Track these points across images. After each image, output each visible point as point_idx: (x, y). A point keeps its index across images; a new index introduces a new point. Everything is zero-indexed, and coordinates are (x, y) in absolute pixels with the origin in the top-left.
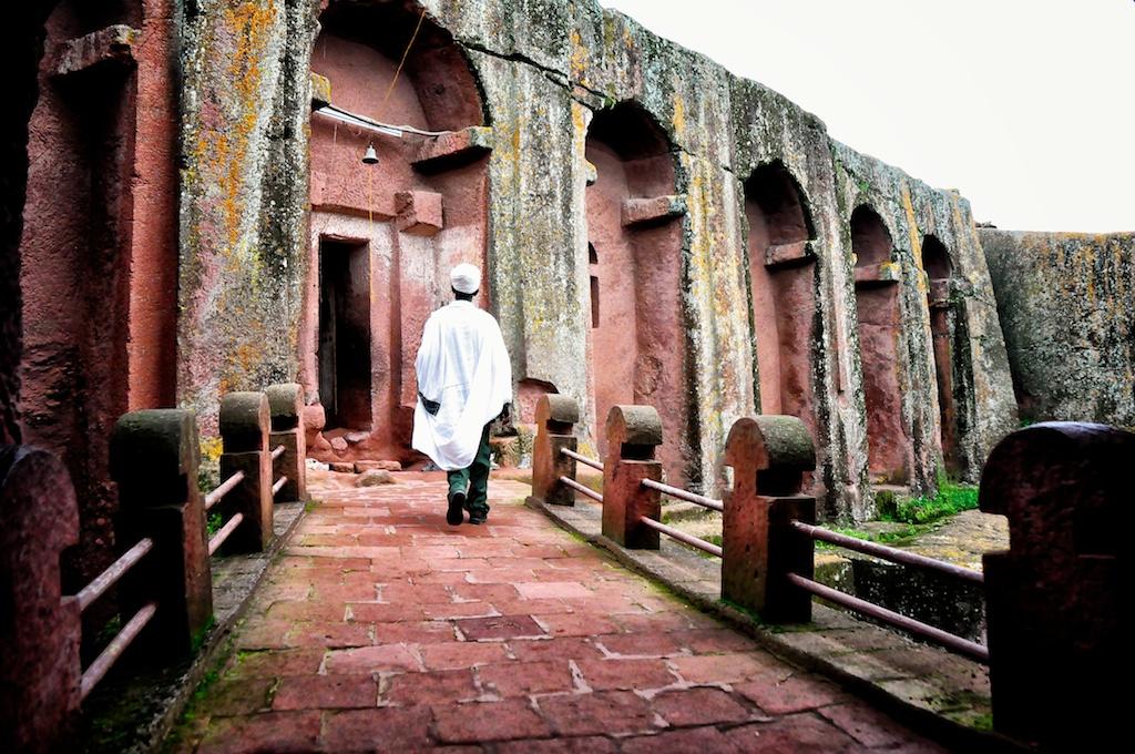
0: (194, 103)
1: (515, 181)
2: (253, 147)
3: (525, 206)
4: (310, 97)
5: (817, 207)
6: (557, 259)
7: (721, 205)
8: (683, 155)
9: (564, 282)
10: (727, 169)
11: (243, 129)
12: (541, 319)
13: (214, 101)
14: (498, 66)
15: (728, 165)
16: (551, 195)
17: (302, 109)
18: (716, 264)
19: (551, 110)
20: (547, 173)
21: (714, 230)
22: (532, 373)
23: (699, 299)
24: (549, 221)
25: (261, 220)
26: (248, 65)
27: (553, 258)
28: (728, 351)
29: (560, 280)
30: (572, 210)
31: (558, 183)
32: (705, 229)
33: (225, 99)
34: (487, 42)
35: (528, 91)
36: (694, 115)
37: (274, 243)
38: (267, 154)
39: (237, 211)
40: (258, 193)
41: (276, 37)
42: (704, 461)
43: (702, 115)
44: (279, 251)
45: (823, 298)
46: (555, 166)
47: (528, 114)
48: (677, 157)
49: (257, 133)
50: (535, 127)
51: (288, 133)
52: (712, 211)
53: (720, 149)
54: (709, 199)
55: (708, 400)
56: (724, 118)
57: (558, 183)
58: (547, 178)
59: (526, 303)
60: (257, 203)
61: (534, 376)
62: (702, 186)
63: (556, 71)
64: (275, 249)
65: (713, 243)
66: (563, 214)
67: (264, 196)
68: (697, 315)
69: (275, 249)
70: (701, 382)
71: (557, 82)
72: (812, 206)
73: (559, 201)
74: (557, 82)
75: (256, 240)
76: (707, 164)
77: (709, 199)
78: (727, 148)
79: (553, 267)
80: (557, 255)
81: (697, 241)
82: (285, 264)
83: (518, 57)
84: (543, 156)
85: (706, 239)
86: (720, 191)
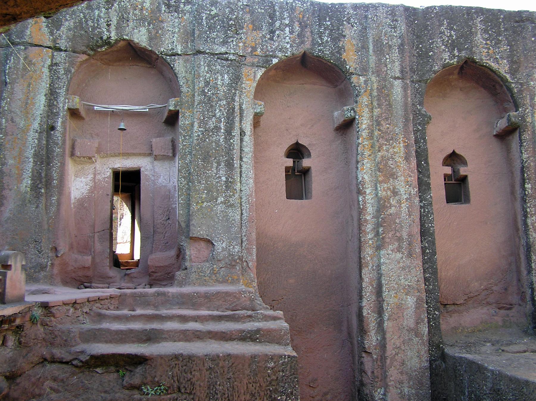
0: (4, 125)
1: (192, 125)
2: (30, 139)
3: (196, 138)
4: (66, 108)
5: (521, 84)
6: (219, 164)
7: (390, 105)
8: (354, 79)
9: (224, 179)
10: (398, 78)
11: (25, 131)
12: (203, 202)
13: (13, 122)
14: (186, 61)
15: (398, 75)
16: (218, 128)
17: (62, 114)
18: (379, 147)
19: (219, 78)
20: (214, 116)
21: (379, 124)
22: (194, 234)
23: (365, 173)
24: (214, 144)
25: (33, 172)
26: (29, 102)
27: (215, 165)
28: (391, 206)
29: (220, 177)
30: (233, 134)
31: (222, 120)
32: (373, 125)
33: (17, 120)
34: (179, 49)
35: (204, 69)
36: (364, 47)
37: (38, 182)
38: (36, 141)
39: (22, 170)
40: (31, 160)
41: (43, 84)
42: (364, 285)
43: (371, 47)
44: (40, 186)
45: (525, 156)
46: (221, 110)
47: (202, 84)
48: (350, 79)
49: (32, 133)
50: (206, 91)
51: (53, 128)
52: (377, 111)
53: (389, 66)
54: (375, 103)
55: (370, 242)
56: (396, 42)
57: (222, 120)
58: (214, 119)
59: (193, 194)
60: (31, 165)
61: (194, 236)
62: (371, 95)
63: (227, 53)
64: (38, 184)
65: (376, 133)
66: (225, 138)
67: (34, 161)
68: (362, 185)
69: (38, 184)
70: (364, 231)
71: (227, 59)
72: (513, 85)
73: (222, 131)
74: (227, 59)
75: (29, 182)
76: (374, 79)
77: (375, 103)
78: (397, 64)
79: (215, 171)
80: (219, 164)
81: (365, 134)
82: (43, 191)
83: (199, 52)
84: (212, 106)
85: (373, 131)
86: (388, 95)
